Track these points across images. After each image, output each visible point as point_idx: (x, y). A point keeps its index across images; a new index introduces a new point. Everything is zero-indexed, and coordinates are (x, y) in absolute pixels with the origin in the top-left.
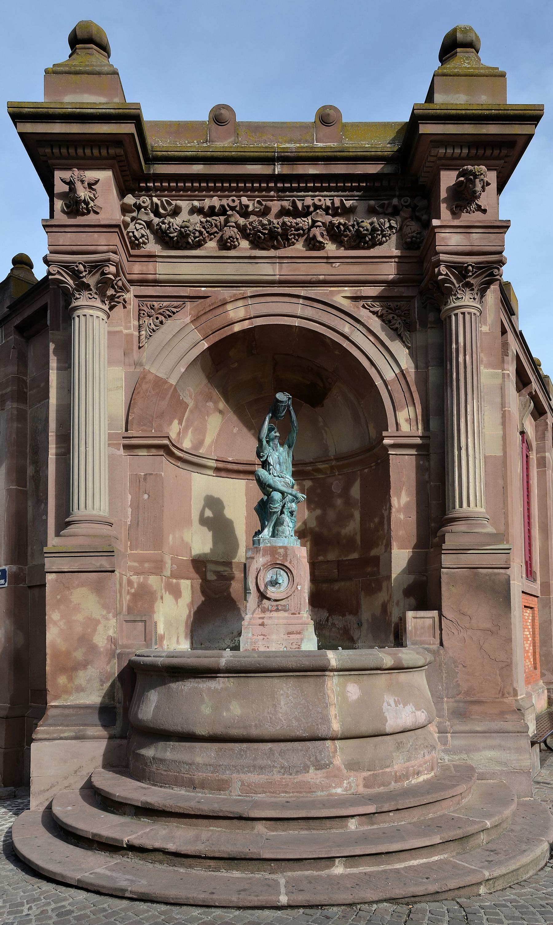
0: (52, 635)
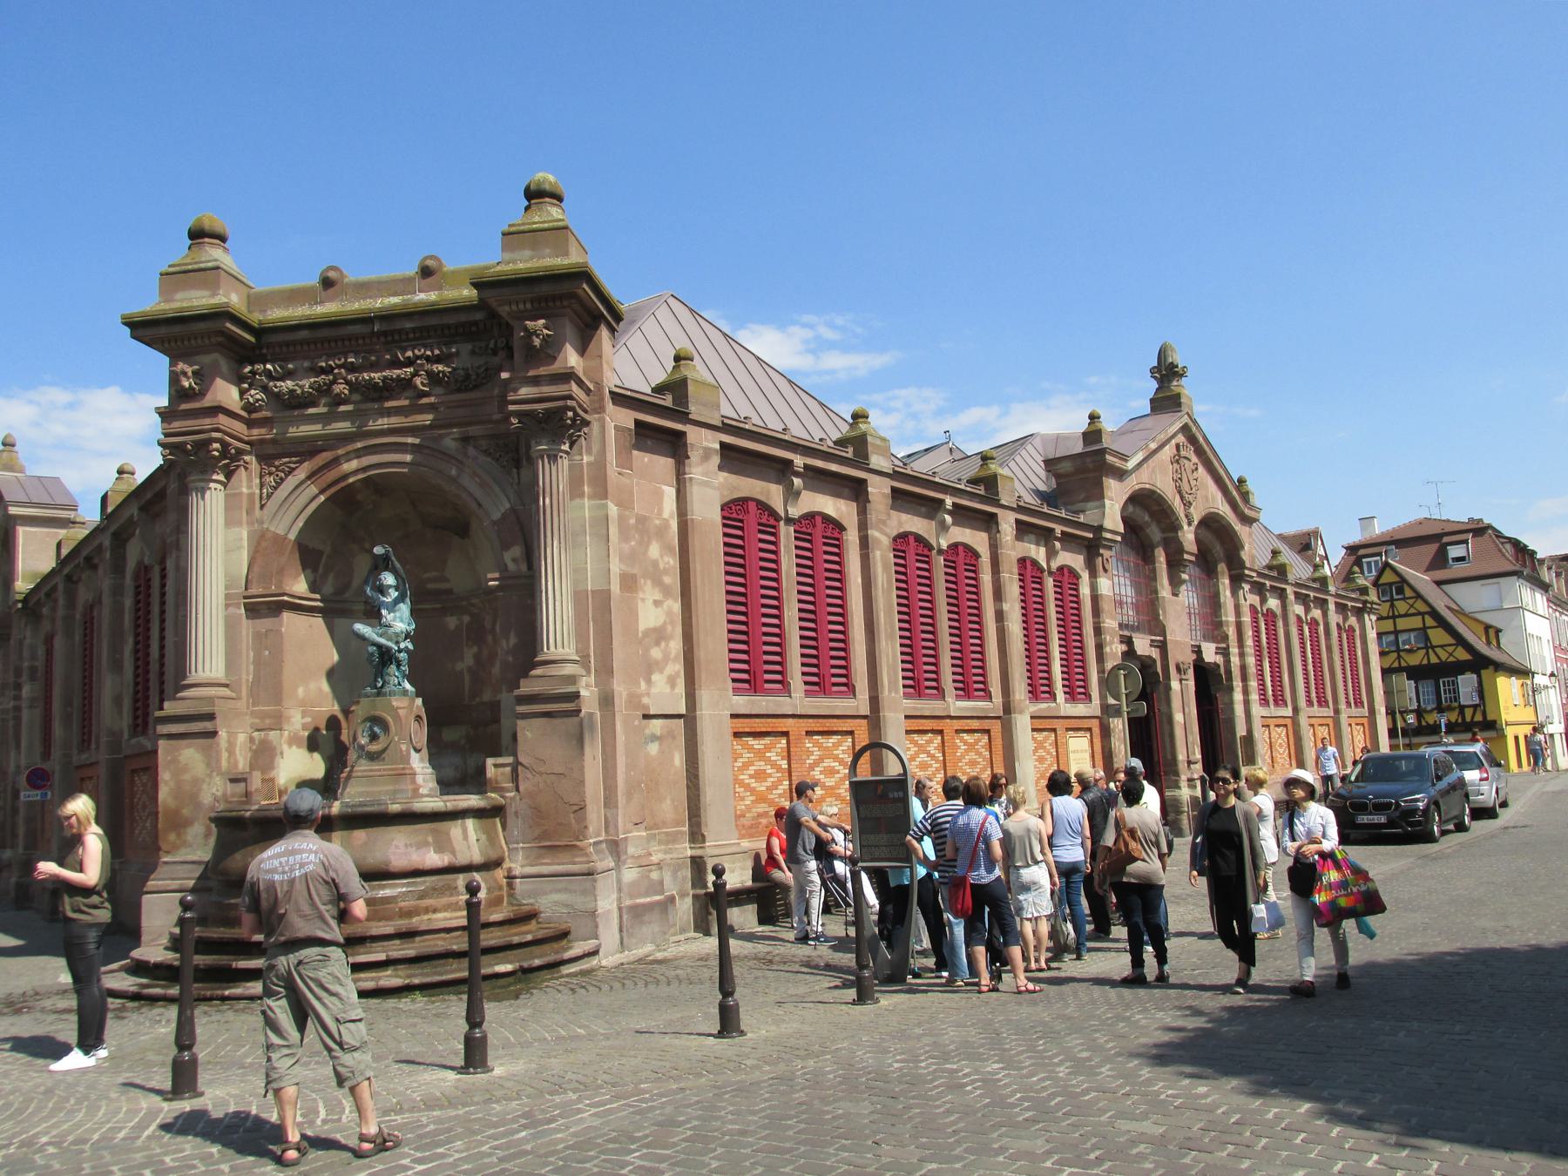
0: (164, 793)
